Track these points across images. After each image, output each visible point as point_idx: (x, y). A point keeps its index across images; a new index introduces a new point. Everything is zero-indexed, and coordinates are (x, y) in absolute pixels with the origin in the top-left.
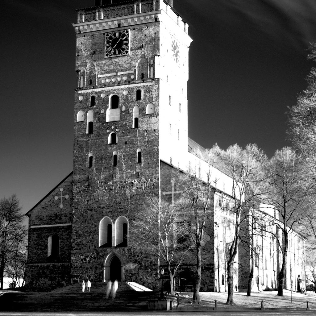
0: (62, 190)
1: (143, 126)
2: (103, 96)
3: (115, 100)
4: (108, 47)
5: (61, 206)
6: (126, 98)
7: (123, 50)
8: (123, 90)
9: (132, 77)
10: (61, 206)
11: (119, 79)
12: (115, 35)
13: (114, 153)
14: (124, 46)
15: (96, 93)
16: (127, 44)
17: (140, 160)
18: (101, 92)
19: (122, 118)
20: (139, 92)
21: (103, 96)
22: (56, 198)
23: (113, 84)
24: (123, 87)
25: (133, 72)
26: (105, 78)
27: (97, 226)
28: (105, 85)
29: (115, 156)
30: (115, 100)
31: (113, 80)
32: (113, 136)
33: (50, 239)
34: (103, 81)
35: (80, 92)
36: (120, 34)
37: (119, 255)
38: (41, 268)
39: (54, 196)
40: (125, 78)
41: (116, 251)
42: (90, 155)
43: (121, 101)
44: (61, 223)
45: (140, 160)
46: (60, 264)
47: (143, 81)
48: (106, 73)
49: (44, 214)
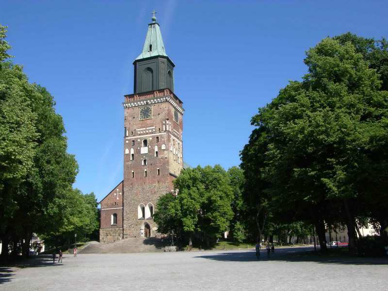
0: (118, 190)
1: (160, 156)
2: (139, 140)
3: (145, 142)
4: (141, 115)
5: (118, 198)
6: (151, 142)
7: (149, 116)
8: (149, 138)
9: (154, 130)
10: (118, 198)
11: (147, 131)
12: (144, 108)
13: (145, 170)
14: (149, 114)
15: (135, 139)
16: (151, 113)
17: (159, 174)
18: (138, 138)
19: (149, 151)
20: (158, 138)
21: (139, 140)
22: (115, 194)
23: (144, 134)
24: (149, 135)
25: (154, 127)
26: (140, 131)
27: (137, 208)
28: (140, 135)
29: (146, 172)
30: (145, 142)
31: (144, 132)
32: (145, 161)
33: (112, 217)
34: (139, 133)
35: (127, 138)
36: (147, 108)
37: (149, 223)
38: (108, 231)
39: (114, 193)
40: (150, 131)
41: (147, 221)
42: (133, 171)
43: (148, 142)
44: (117, 207)
45: (159, 174)
46: (117, 229)
47: (160, 132)
48: (141, 128)
49: (109, 202)
